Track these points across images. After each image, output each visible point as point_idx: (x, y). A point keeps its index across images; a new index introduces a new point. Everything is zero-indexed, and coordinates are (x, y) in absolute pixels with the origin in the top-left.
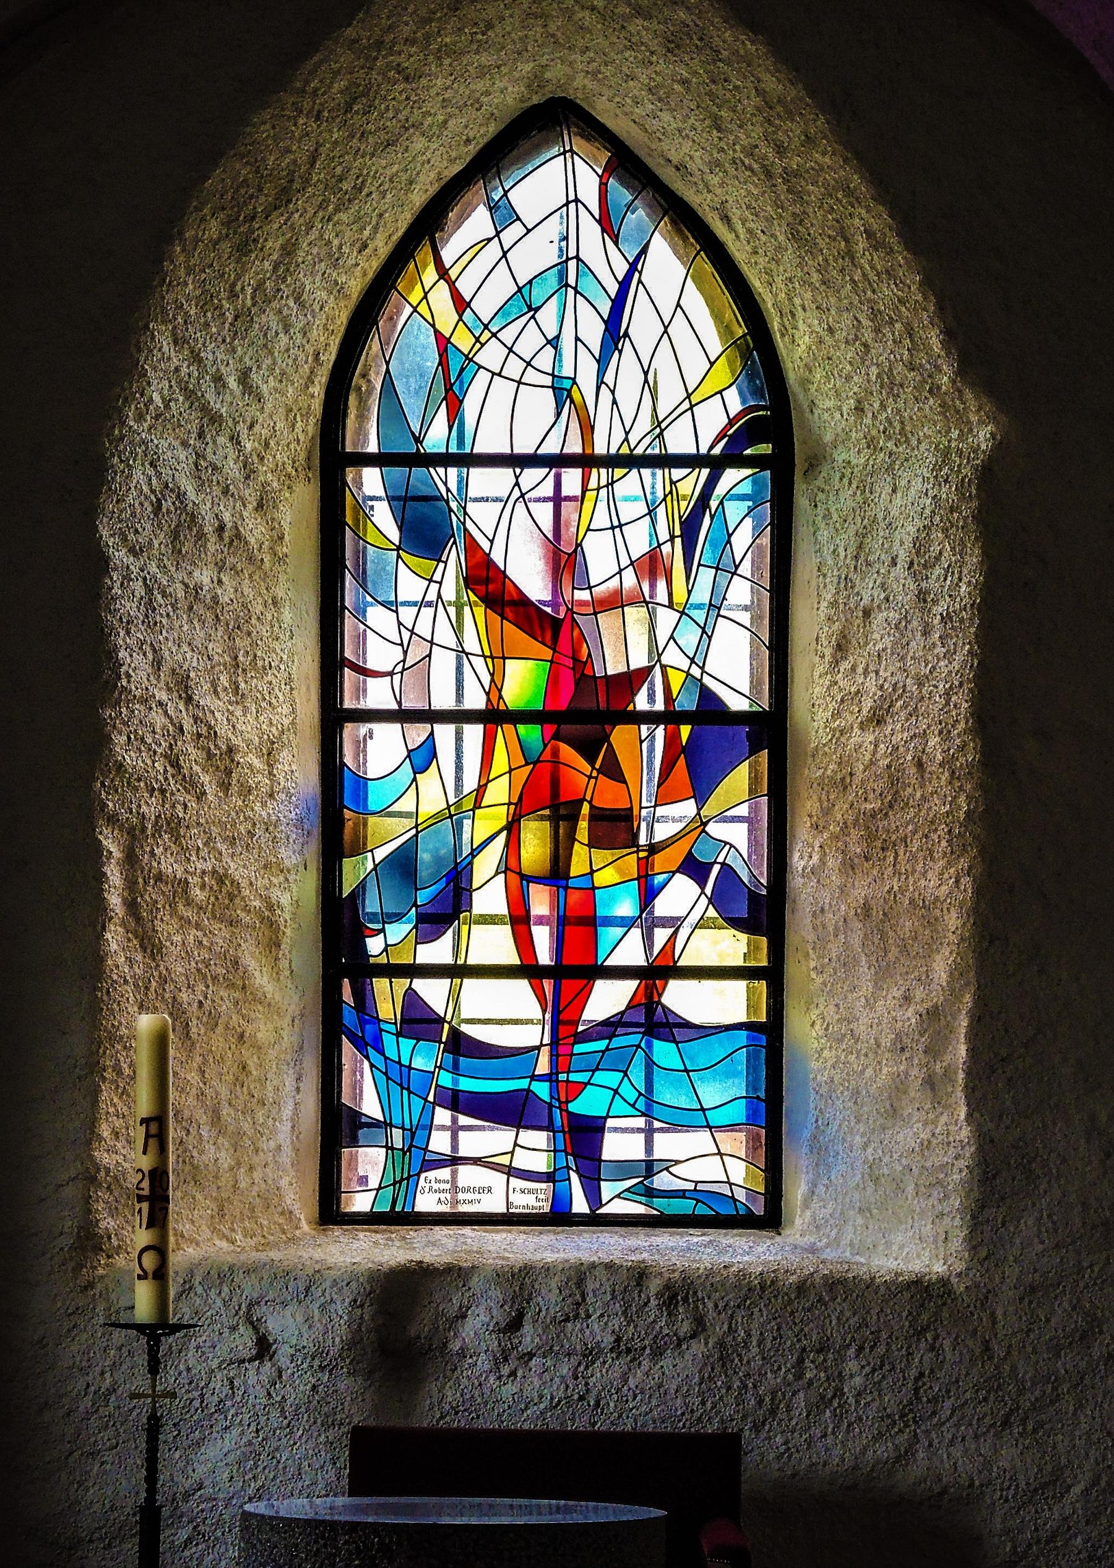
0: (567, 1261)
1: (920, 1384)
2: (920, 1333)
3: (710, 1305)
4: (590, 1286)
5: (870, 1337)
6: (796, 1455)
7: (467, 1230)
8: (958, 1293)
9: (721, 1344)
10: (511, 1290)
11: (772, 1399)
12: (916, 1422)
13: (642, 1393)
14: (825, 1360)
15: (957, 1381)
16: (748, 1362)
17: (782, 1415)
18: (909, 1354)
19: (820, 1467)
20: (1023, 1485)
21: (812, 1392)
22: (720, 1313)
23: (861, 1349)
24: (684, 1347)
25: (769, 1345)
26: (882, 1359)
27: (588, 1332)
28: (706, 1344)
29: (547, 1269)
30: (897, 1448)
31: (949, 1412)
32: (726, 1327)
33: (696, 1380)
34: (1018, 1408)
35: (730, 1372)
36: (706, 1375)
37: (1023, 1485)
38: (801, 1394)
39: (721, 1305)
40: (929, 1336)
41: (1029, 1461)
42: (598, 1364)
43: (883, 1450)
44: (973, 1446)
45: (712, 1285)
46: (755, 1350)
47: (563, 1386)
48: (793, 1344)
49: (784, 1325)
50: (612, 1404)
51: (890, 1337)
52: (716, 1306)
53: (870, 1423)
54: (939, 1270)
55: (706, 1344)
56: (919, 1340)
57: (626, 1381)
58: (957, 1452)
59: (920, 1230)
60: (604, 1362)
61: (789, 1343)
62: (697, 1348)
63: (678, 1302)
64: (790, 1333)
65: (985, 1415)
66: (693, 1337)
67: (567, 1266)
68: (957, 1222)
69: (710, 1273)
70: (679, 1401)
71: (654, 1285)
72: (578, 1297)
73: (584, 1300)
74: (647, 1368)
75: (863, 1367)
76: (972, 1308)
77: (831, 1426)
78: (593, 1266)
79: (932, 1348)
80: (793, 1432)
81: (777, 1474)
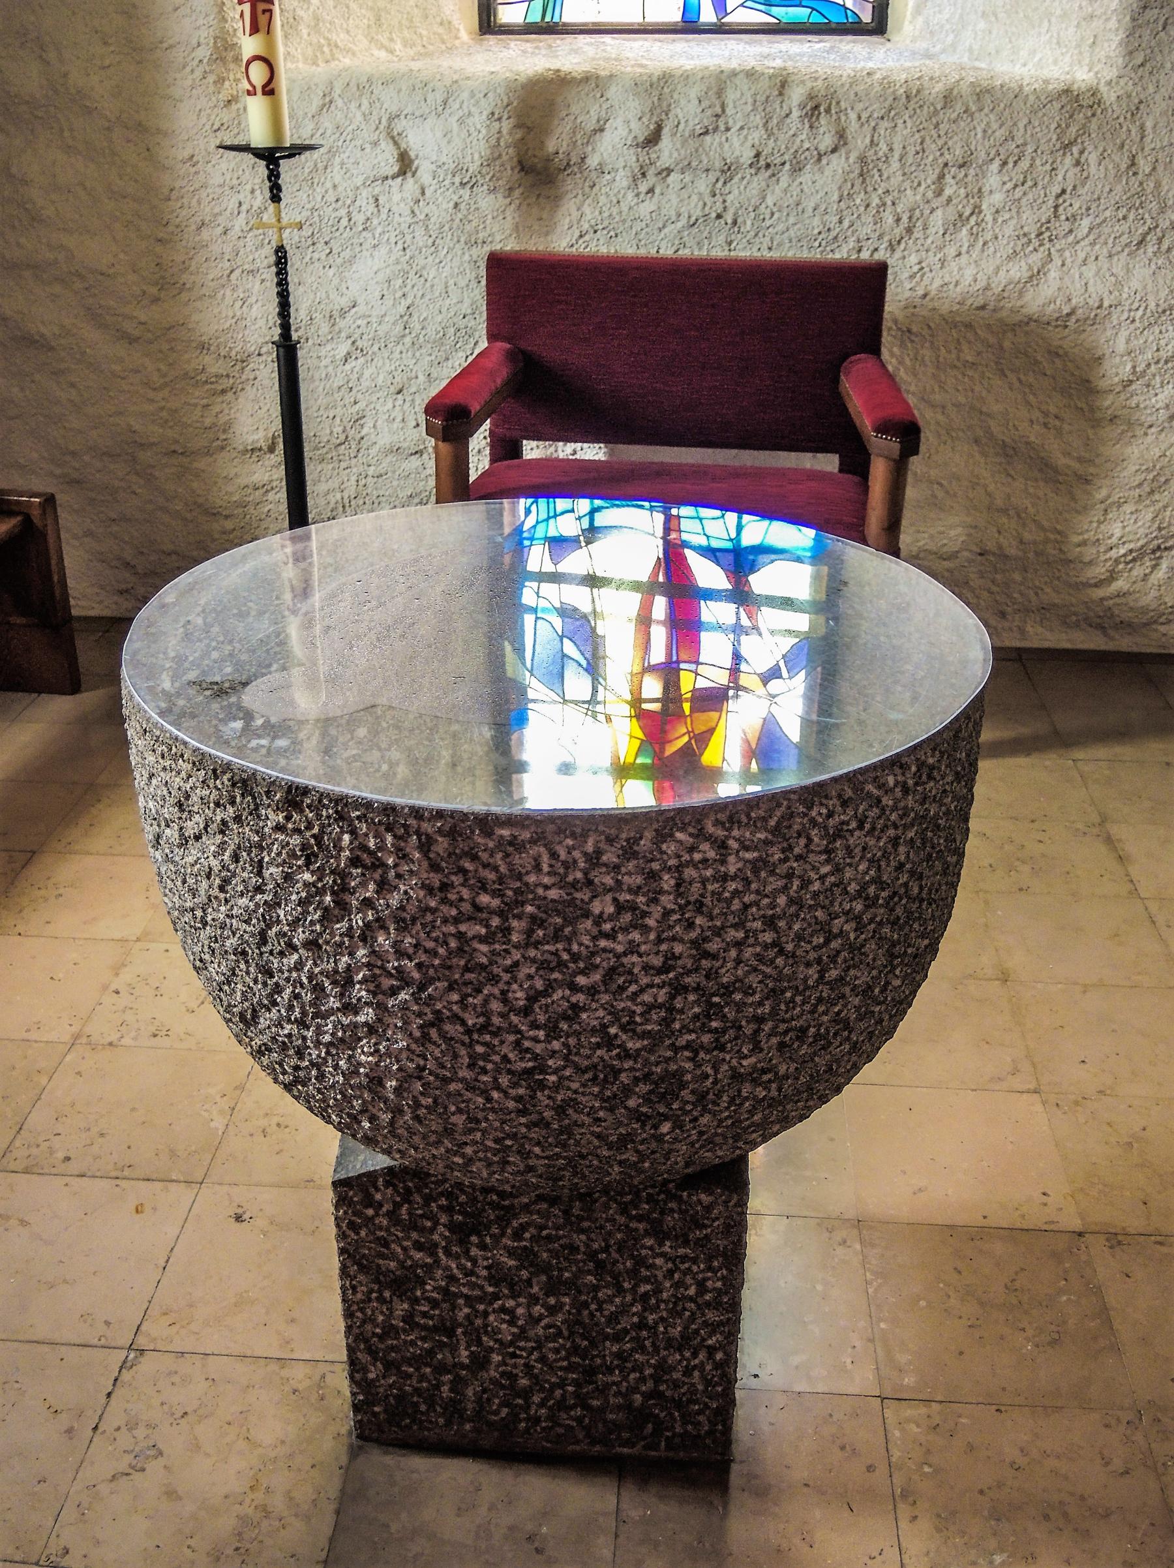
0: (707, 68)
1: (1061, 201)
2: (1067, 147)
3: (853, 116)
4: (731, 96)
5: (1016, 151)
6: (929, 274)
7: (607, 38)
8: (1108, 103)
9: (862, 160)
10: (650, 102)
11: (910, 218)
12: (1051, 240)
13: (779, 211)
14: (966, 176)
15: (1099, 199)
16: (888, 178)
17: (918, 233)
18: (1053, 169)
19: (951, 287)
20: (1152, 305)
21: (951, 209)
22: (862, 125)
23: (1005, 163)
24: (824, 161)
25: (910, 160)
26: (1025, 174)
27: (727, 146)
28: (847, 158)
29: (686, 77)
30: (1030, 268)
31: (1086, 230)
32: (868, 141)
33: (836, 197)
34: (1157, 226)
35: (870, 189)
36: (846, 193)
37: (1152, 305)
38: (939, 212)
39: (864, 116)
40: (1075, 150)
41: (1161, 281)
42: (736, 179)
43: (1018, 271)
44: (1106, 266)
45: (856, 94)
46: (895, 165)
47: (701, 203)
48: (935, 159)
49: (928, 138)
50: (749, 223)
51: (1035, 151)
52: (859, 118)
53: (1005, 242)
54: (1085, 77)
55: (847, 158)
56: (1064, 154)
57: (764, 198)
58: (1090, 272)
59: (1058, 34)
60: (743, 178)
61: (931, 158)
62: (837, 164)
63: (820, 114)
64: (934, 146)
65: (1123, 234)
66: (834, 151)
67: (707, 73)
68: (1113, 24)
69: (854, 81)
70: (816, 218)
71: (796, 95)
72: (718, 110)
73: (724, 111)
74: (786, 185)
75: (1004, 183)
76: (1122, 120)
77: (966, 245)
78: (734, 74)
79: (1078, 163)
80: (927, 251)
81: (908, 294)
